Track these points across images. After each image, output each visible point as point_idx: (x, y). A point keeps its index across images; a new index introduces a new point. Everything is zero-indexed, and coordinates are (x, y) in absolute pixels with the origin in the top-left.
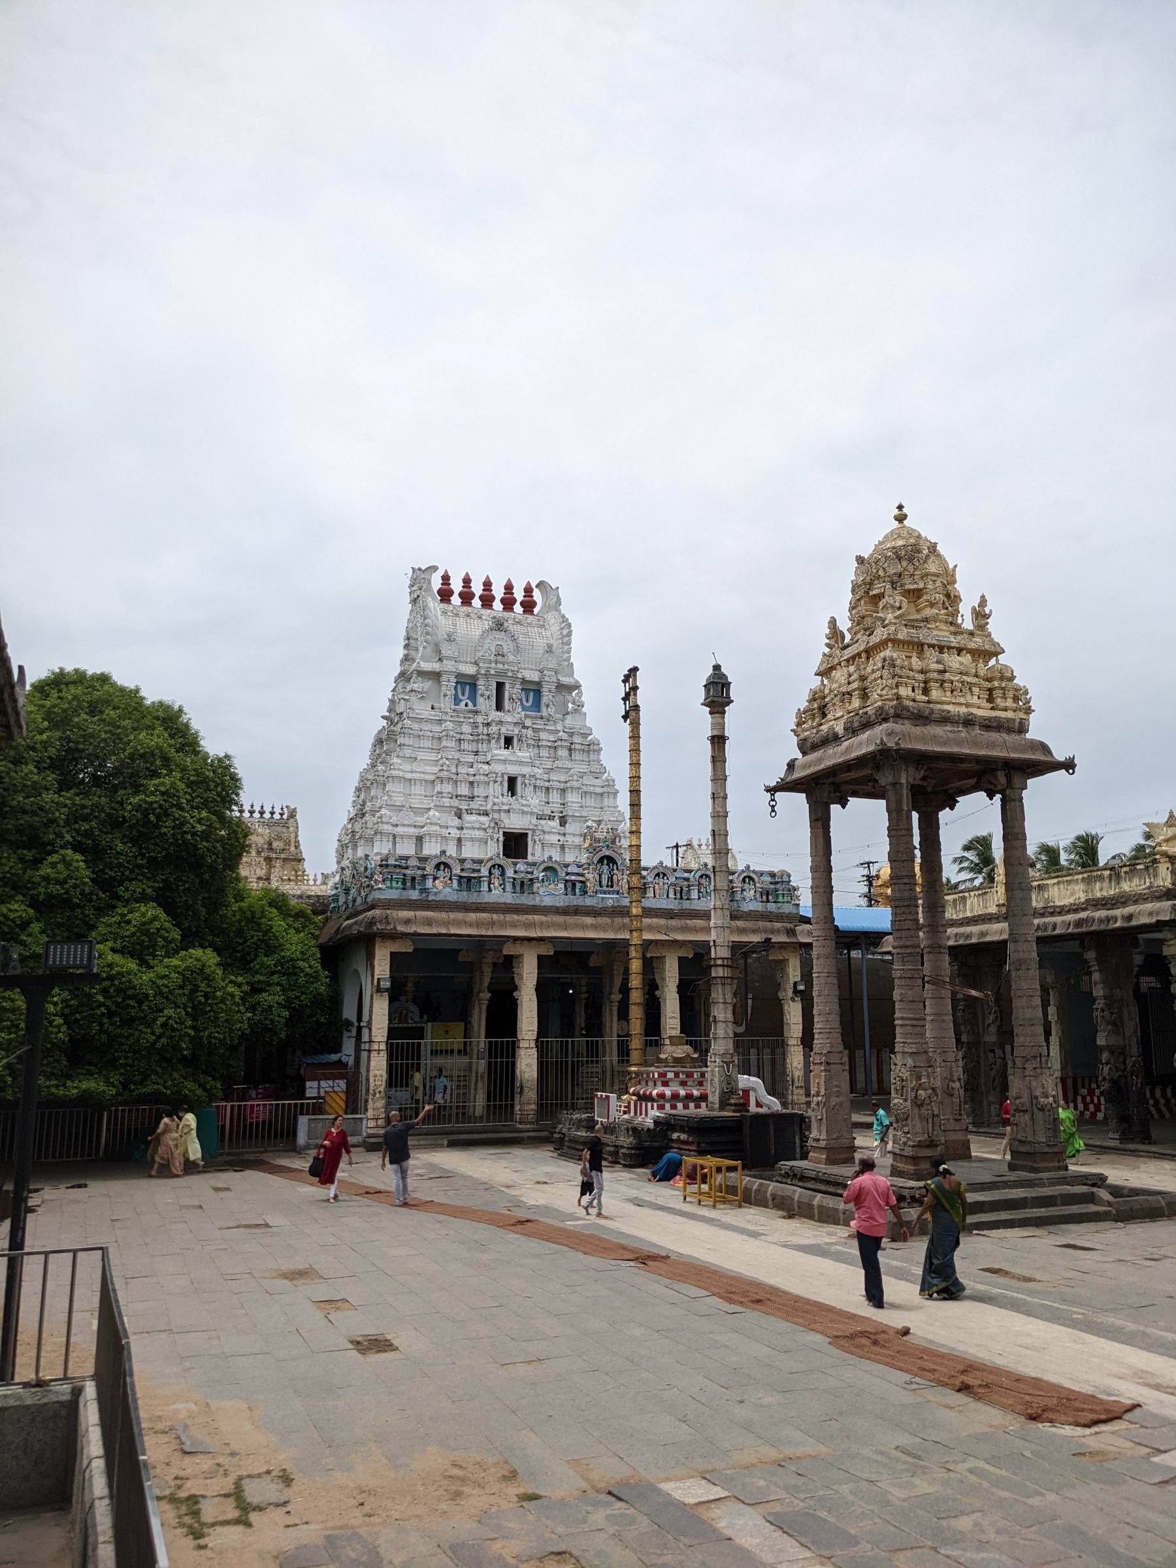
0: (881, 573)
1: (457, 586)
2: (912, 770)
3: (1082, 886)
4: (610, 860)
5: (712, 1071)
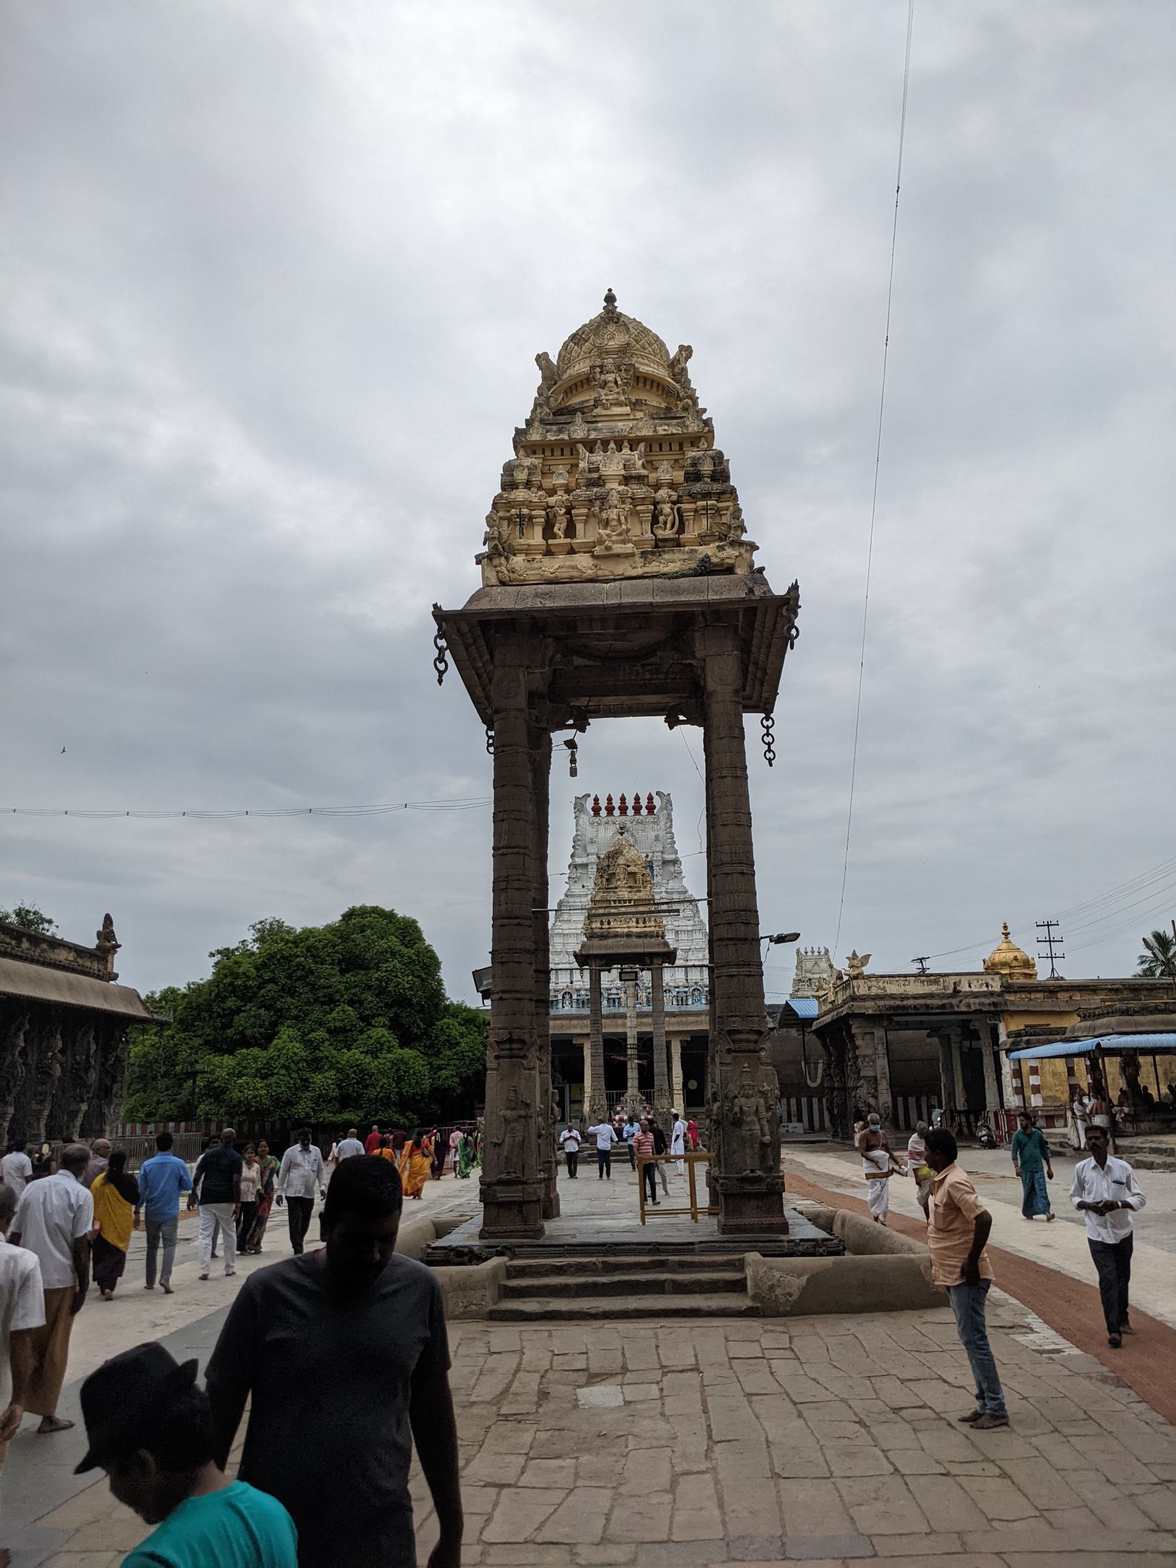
1: (603, 803)
2: (598, 962)
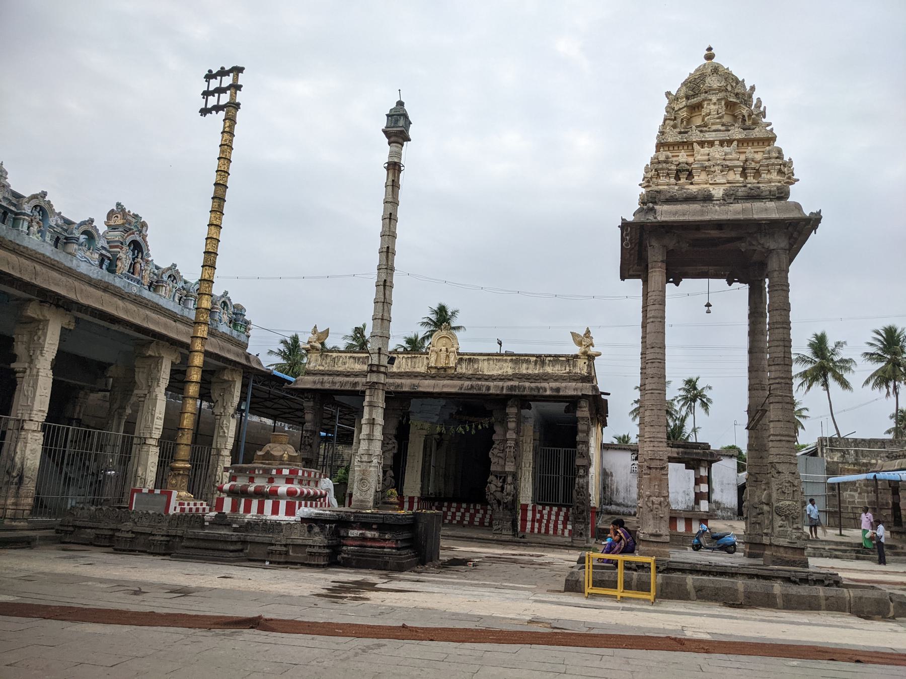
0: (729, 88)
3: (510, 365)
4: (138, 247)
5: (364, 472)
